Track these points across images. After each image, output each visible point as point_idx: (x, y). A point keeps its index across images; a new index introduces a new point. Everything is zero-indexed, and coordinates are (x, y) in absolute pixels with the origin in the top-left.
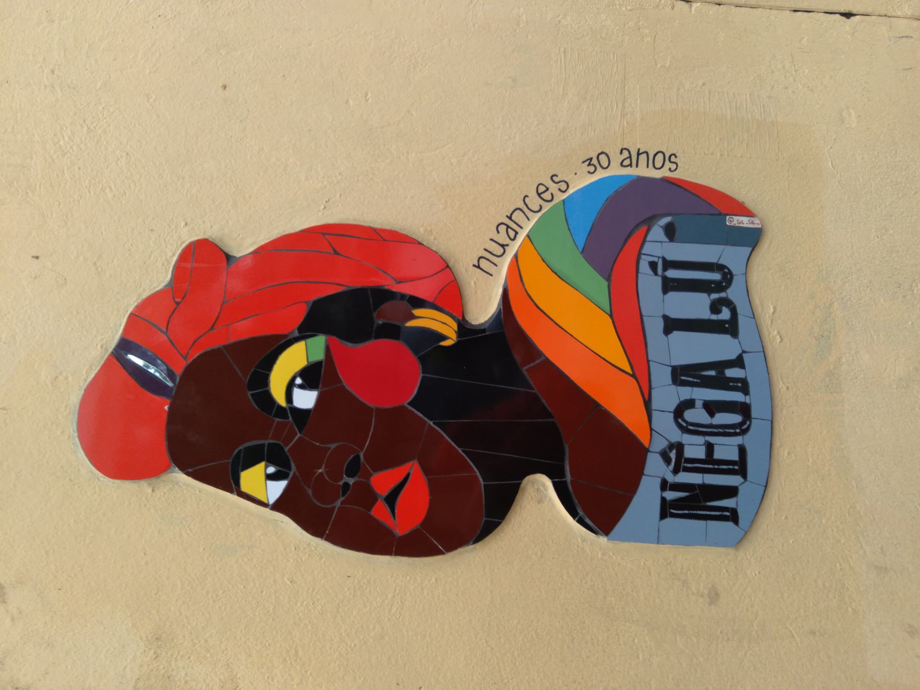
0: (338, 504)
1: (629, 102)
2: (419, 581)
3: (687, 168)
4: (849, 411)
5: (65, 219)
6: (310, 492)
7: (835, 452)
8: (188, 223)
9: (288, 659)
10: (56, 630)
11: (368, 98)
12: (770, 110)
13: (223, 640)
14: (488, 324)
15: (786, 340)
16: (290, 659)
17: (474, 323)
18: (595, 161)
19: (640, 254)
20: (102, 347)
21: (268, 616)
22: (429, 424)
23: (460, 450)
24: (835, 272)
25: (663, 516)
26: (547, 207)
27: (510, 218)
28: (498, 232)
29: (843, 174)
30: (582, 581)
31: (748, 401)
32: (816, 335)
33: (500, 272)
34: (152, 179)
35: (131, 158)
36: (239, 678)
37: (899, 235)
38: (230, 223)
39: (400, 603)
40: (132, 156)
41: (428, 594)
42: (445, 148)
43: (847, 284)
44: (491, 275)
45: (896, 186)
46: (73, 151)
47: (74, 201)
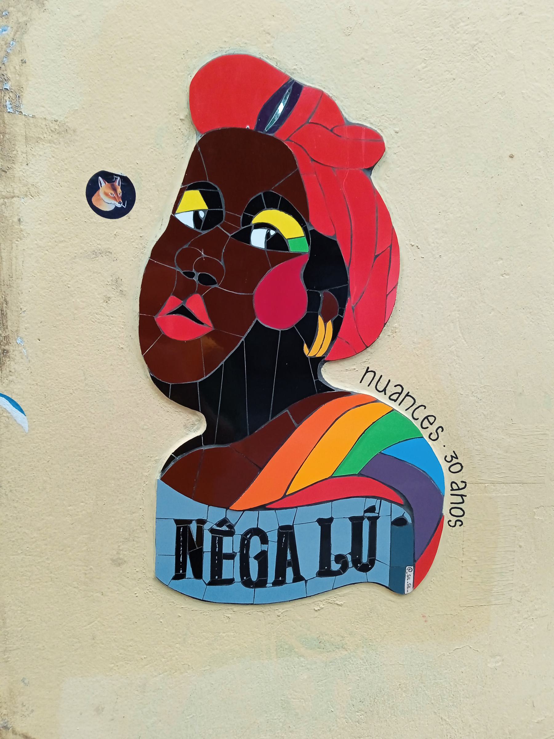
0: (178, 269)
1: (505, 487)
2: (120, 335)
3: (452, 534)
4: (263, 663)
5: (399, 32)
6: (186, 246)
7: (231, 653)
8: (397, 134)
9: (56, 235)
10: (70, 50)
11: (504, 275)
12: (500, 599)
13: (68, 183)
14: (321, 381)
15: (316, 614)
16: (56, 237)
17: (322, 369)
18: (455, 461)
19: (381, 499)
20: (295, 69)
21: (88, 218)
22: (242, 338)
23: (223, 363)
24: (371, 652)
25: (177, 522)
26: (417, 424)
27: (407, 395)
28: (395, 386)
29: (450, 657)
30: (125, 461)
31: (267, 585)
32: (321, 637)
33: (364, 389)
34: (434, 101)
35: (451, 82)
36: (39, 198)
37: (402, 701)
38: (398, 169)
39: (103, 321)
40: (452, 83)
41: (111, 342)
42: (463, 340)
43: (361, 661)
44: (361, 382)
45: (440, 699)
46: (455, 34)
47: (414, 37)
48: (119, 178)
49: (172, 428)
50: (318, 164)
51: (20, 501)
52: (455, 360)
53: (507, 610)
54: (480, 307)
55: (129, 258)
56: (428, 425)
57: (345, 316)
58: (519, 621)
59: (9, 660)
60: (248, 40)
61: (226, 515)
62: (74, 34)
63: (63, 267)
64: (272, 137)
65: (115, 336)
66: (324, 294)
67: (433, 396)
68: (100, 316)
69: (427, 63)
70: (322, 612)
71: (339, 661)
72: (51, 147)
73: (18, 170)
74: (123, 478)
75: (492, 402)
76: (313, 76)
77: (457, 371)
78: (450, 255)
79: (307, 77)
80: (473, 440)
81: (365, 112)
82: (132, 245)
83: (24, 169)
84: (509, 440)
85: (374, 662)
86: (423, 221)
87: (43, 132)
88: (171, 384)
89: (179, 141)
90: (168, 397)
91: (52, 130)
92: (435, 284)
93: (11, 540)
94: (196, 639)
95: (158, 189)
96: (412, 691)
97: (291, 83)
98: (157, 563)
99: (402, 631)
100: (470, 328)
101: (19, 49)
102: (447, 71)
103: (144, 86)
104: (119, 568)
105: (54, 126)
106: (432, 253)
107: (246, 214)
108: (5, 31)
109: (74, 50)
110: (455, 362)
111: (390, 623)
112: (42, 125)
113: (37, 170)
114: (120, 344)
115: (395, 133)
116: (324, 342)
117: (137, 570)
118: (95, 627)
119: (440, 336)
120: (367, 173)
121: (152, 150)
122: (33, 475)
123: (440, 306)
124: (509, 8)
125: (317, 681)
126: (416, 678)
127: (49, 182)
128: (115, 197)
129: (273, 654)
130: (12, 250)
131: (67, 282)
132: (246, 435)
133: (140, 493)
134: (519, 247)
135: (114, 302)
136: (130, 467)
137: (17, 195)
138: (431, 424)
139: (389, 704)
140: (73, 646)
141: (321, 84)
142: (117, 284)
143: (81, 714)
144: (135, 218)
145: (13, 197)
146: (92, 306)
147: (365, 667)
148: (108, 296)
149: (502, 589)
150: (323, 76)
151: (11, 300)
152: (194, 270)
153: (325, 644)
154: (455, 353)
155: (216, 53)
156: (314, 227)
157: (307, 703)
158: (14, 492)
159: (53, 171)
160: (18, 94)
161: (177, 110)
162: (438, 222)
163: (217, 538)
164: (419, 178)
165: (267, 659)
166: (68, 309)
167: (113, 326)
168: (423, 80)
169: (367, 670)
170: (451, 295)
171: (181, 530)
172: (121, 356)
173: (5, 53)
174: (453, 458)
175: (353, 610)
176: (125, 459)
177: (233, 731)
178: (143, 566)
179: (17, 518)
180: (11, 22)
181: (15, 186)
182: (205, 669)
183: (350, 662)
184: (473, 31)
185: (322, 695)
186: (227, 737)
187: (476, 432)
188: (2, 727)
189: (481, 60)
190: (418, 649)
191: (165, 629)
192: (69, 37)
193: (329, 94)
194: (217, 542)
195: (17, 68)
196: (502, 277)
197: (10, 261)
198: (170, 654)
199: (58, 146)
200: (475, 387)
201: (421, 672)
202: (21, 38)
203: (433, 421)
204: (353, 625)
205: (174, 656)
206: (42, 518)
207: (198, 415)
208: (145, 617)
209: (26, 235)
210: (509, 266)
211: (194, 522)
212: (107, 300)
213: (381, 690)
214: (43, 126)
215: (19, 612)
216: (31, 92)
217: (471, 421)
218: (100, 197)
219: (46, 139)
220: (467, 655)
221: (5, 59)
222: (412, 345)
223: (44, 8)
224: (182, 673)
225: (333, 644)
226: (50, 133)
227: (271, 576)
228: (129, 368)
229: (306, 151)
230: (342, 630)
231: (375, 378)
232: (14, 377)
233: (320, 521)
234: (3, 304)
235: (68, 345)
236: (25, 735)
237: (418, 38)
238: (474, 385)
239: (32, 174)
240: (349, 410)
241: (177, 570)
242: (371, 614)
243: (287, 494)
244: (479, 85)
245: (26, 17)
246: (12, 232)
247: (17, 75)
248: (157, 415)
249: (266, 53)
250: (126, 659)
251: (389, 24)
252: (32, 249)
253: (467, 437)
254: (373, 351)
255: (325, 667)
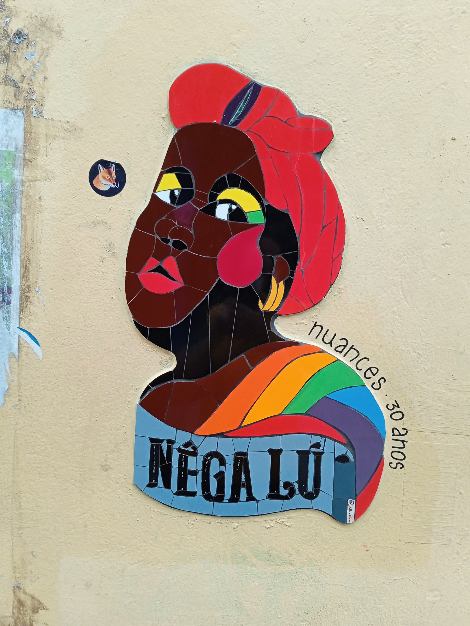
0: (157, 236)
1: (445, 437)
2: (112, 288)
3: (393, 475)
4: (220, 567)
5: (348, 36)
6: (163, 218)
7: (193, 554)
8: (346, 123)
9: (66, 209)
10: (80, 67)
11: (446, 245)
12: (440, 540)
13: (76, 170)
14: (274, 332)
15: (267, 531)
16: (66, 211)
17: (275, 322)
18: (396, 409)
19: (326, 437)
20: (256, 73)
21: (90, 196)
22: (207, 293)
23: (191, 313)
24: (315, 571)
25: (152, 440)
26: (360, 374)
27: (352, 348)
28: (341, 340)
29: (389, 586)
30: (113, 387)
31: (224, 501)
32: (271, 552)
33: (312, 340)
34: (379, 94)
35: (395, 76)
36: (55, 181)
37: (343, 618)
38: (346, 152)
39: (99, 276)
40: (397, 77)
41: (105, 293)
42: (405, 302)
43: (307, 578)
44: (309, 334)
45: (380, 621)
46: (400, 35)
47: (362, 40)
48: (114, 165)
49: (150, 364)
50: (274, 150)
51: (34, 412)
52: (397, 319)
53: (446, 550)
54: (422, 272)
55: (120, 227)
56: (371, 375)
57: (295, 278)
58: (459, 562)
59: (22, 535)
60: (217, 52)
61: (191, 439)
62: (83, 55)
63: (70, 234)
64: (235, 129)
65: (108, 288)
66: (277, 258)
67: (375, 350)
68: (96, 272)
69: (373, 61)
70: (272, 530)
71: (287, 575)
72: (64, 142)
73: (40, 160)
74: (111, 401)
75: (433, 358)
76: (271, 78)
77: (399, 329)
78: (394, 226)
79: (266, 79)
80: (415, 392)
81: (316, 105)
82: (123, 217)
83: (44, 159)
84: (450, 395)
85: (318, 580)
86: (368, 197)
87: (58, 131)
88: (149, 328)
89: (160, 135)
90: (147, 339)
91: (65, 130)
92: (379, 252)
93: (27, 442)
94: (165, 538)
95: (144, 173)
96: (353, 611)
97: (252, 85)
98: (135, 472)
99: (345, 556)
100: (412, 292)
101: (42, 68)
102: (392, 67)
103: (134, 92)
104: (106, 472)
105: (66, 126)
106: (376, 225)
107: (212, 192)
108: (33, 55)
109: (83, 67)
110: (398, 321)
111: (333, 548)
112: (58, 126)
113: (54, 160)
114: (111, 295)
115: (343, 122)
116: (276, 299)
117: (120, 476)
118: (87, 517)
119: (383, 297)
120: (317, 157)
121: (140, 142)
122: (45, 393)
123: (383, 271)
124: (452, 9)
125: (267, 589)
126: (357, 600)
127: (62, 169)
128: (110, 180)
129: (229, 560)
130: (34, 220)
131: (73, 246)
132: (208, 373)
133: (124, 414)
134: (461, 220)
135: (108, 261)
136: (117, 392)
137: (39, 179)
138: (374, 375)
139: (331, 619)
140: (70, 530)
141: (278, 83)
142: (111, 247)
143: (74, 586)
144: (126, 196)
145: (36, 181)
146: (91, 264)
147: (310, 583)
148: (103, 256)
149: (442, 531)
150: (280, 77)
151: (32, 259)
152: (169, 237)
153: (274, 558)
154: (397, 313)
155: (191, 63)
156: (269, 203)
157: (257, 607)
158: (31, 405)
159: (65, 161)
160: (41, 103)
161: (159, 110)
162: (382, 197)
163: (183, 457)
164: (365, 160)
165: (224, 563)
166: (73, 266)
167: (107, 280)
168: (369, 76)
169: (312, 586)
170: (394, 261)
171: (155, 447)
172: (111, 304)
173: (33, 72)
174: (395, 407)
175: (300, 532)
176: (113, 386)
177: (194, 620)
178: (125, 473)
179: (32, 426)
180: (37, 49)
181: (38, 172)
182: (172, 564)
183: (296, 577)
184: (417, 31)
185: (271, 602)
186: (189, 624)
187: (417, 385)
188: (16, 587)
189: (424, 56)
190: (360, 575)
191: (141, 527)
192: (79, 58)
193: (285, 92)
194: (183, 460)
195: (40, 83)
196: (444, 247)
197: (33, 228)
198: (145, 548)
199: (69, 141)
200: (417, 344)
201: (362, 596)
202: (44, 61)
203: (376, 372)
204: (299, 545)
205: (147, 550)
206: (50, 427)
207: (170, 355)
208: (125, 514)
209: (44, 209)
210: (451, 237)
211: (165, 442)
212: (103, 260)
213: (324, 606)
214: (59, 127)
215: (31, 498)
216: (51, 101)
217: (412, 374)
218: (99, 180)
219: (61, 136)
220: (406, 586)
221: (32, 77)
222: (357, 305)
223: (61, 37)
224: (153, 565)
225: (281, 559)
226: (63, 131)
227: (228, 493)
228: (118, 314)
229: (264, 141)
230: (289, 547)
231: (322, 331)
232: (33, 317)
233: (271, 451)
234: (26, 261)
235: (72, 294)
236: (32, 595)
237: (365, 41)
238: (415, 342)
239: (50, 163)
240: (297, 358)
241: (151, 479)
242: (316, 537)
243: (242, 426)
244: (423, 78)
245: (48, 44)
246: (34, 207)
247: (41, 89)
248: (138, 352)
249: (232, 61)
250: (110, 547)
251: (339, 31)
252: (48, 220)
253: (409, 389)
254: (321, 308)
255: (273, 578)
